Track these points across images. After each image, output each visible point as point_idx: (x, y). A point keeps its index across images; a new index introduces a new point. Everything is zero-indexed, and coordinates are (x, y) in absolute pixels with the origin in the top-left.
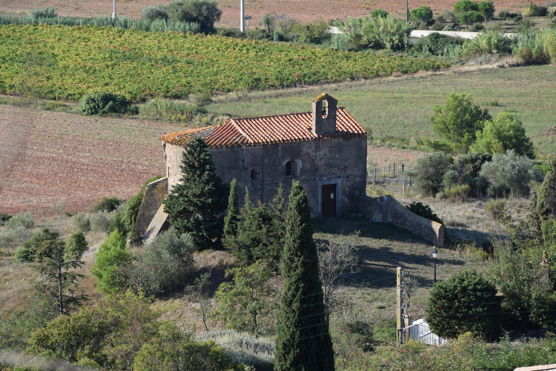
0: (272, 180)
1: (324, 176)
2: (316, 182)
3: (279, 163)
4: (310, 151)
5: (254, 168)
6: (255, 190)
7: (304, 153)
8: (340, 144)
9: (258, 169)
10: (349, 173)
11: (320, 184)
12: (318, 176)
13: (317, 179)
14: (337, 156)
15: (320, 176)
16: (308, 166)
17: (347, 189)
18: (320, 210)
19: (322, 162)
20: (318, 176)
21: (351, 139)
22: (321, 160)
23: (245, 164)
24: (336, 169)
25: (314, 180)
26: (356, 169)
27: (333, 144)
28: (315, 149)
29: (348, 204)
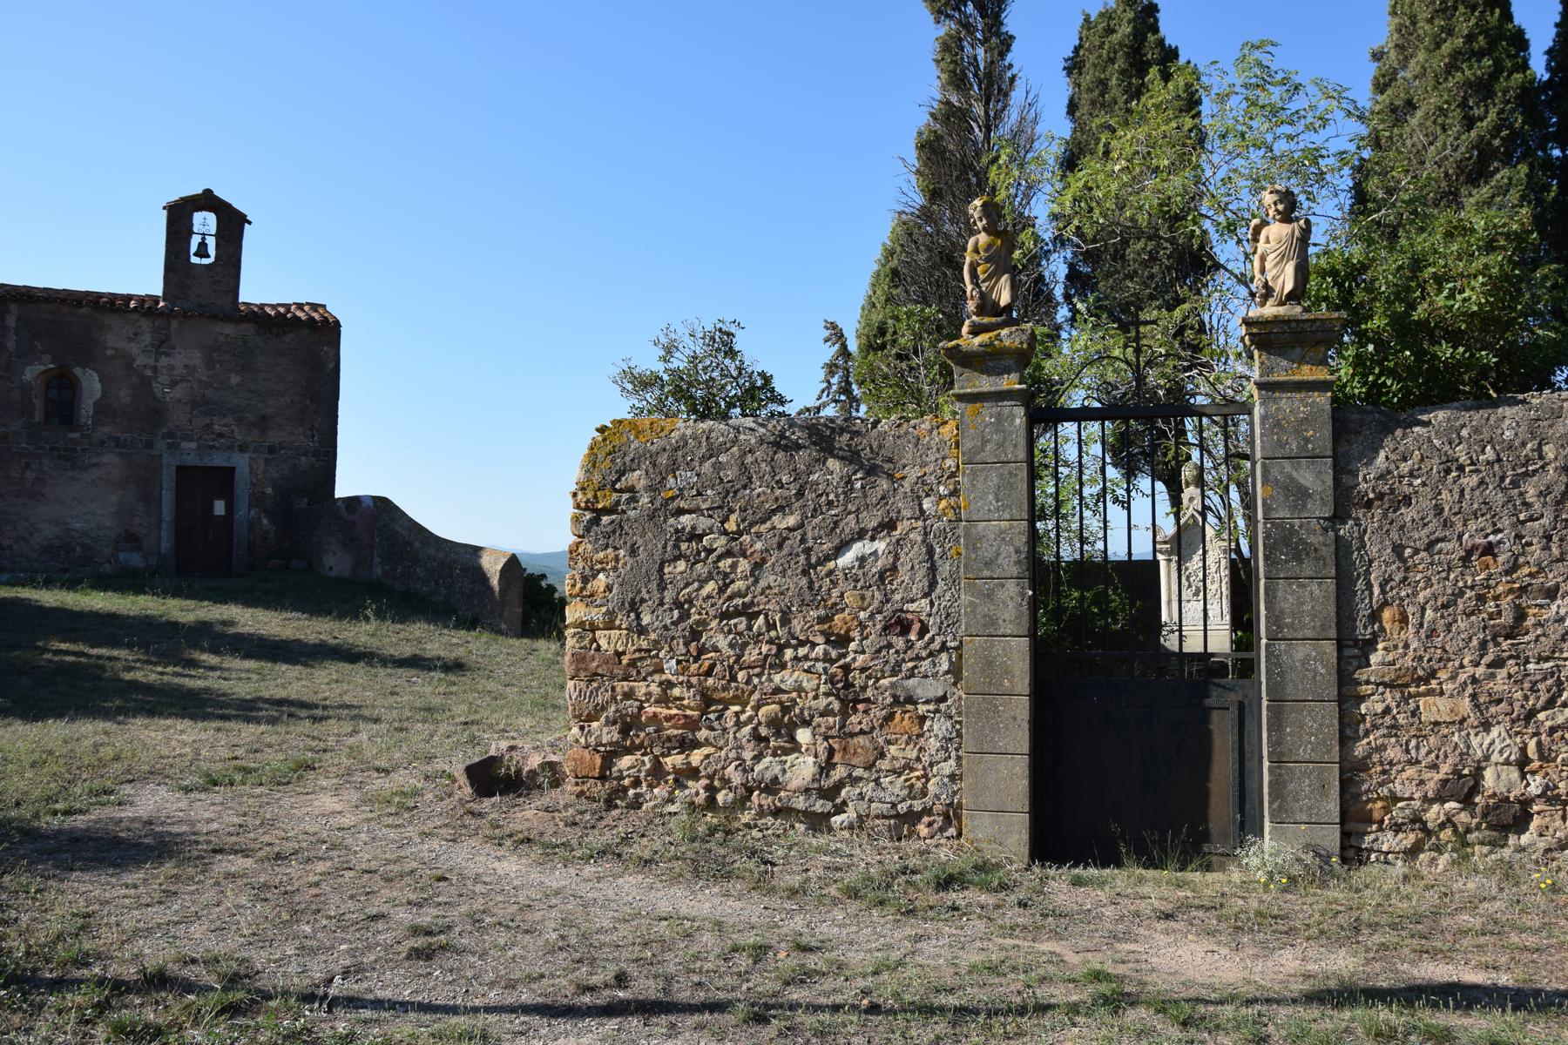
1: (188, 438)
4: (133, 348)
7: (109, 352)
8: (245, 343)
10: (274, 437)
11: (169, 462)
13: (160, 444)
14: (235, 379)
15: (171, 435)
16: (124, 395)
17: (269, 490)
18: (166, 545)
19: (180, 392)
22: (174, 384)
24: (230, 420)
25: (149, 445)
27: (221, 338)
28: (152, 345)
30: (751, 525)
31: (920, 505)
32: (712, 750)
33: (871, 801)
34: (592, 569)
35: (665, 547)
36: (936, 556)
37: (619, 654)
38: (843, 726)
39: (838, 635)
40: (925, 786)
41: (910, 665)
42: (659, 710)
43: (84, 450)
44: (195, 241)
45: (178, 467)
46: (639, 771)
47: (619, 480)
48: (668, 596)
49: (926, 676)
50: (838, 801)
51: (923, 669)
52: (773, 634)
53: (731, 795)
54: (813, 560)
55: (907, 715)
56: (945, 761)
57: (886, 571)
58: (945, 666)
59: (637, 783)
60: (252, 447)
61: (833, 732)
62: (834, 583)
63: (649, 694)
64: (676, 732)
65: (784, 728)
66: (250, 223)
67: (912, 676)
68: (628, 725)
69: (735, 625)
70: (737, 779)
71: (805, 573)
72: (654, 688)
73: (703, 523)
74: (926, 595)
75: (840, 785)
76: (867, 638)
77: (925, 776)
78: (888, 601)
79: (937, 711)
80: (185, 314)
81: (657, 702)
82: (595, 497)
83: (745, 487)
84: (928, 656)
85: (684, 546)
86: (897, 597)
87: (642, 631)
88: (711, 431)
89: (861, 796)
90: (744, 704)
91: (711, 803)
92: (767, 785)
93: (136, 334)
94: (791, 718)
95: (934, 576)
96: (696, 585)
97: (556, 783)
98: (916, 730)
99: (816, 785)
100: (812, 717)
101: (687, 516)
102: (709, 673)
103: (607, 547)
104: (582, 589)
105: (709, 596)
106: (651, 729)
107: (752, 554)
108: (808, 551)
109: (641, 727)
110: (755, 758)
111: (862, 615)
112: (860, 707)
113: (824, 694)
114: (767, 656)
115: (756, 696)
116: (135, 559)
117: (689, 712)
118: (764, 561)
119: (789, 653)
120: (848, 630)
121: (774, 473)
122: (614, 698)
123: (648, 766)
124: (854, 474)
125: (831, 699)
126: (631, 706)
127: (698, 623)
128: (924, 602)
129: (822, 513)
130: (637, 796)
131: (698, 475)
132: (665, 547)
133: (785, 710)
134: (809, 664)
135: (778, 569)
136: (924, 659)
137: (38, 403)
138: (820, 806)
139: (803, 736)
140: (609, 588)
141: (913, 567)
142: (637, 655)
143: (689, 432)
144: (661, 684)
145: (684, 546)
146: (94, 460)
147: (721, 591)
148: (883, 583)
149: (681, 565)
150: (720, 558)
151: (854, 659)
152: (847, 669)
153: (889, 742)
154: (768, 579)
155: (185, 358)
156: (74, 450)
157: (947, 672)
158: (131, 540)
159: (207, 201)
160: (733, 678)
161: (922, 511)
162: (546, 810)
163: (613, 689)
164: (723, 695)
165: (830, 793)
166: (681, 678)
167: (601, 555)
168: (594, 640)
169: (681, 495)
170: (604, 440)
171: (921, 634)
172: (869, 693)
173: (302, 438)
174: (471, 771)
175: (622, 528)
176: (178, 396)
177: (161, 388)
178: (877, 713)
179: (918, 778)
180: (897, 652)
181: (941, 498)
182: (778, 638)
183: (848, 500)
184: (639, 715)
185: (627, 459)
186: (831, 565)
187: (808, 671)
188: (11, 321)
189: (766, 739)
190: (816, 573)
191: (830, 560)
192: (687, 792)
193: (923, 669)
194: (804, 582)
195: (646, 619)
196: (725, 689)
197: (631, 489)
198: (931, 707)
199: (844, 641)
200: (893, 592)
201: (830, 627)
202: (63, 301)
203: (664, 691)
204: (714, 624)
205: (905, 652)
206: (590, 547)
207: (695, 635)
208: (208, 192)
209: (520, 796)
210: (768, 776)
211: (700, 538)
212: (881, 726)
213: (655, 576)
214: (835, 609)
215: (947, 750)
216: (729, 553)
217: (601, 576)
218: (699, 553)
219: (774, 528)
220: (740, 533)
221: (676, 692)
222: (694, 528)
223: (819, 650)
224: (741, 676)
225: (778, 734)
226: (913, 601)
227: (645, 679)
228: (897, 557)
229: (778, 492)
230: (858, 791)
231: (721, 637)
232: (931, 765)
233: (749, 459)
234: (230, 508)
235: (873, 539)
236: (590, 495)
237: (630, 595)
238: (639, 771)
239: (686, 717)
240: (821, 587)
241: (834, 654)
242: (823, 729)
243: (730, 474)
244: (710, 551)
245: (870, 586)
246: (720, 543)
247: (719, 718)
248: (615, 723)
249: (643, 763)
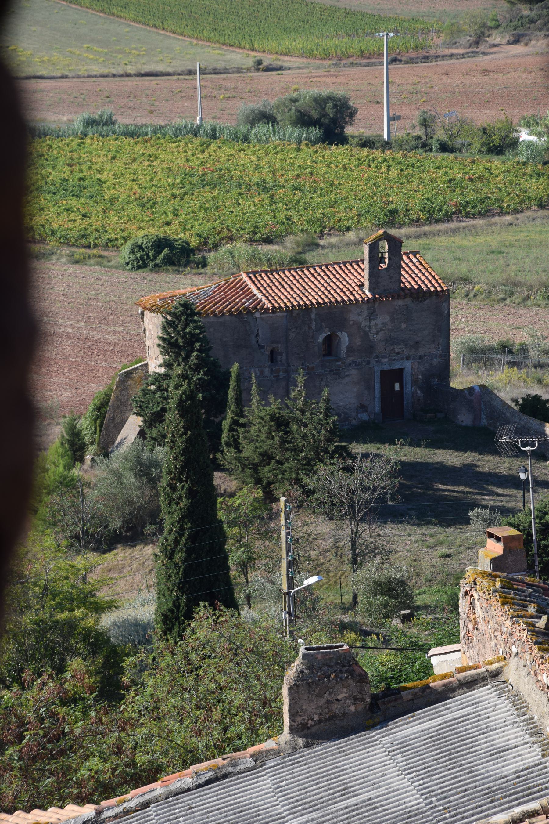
1: (384, 357)
2: (371, 366)
4: (361, 319)
5: (275, 345)
7: (351, 323)
8: (407, 307)
9: (280, 348)
11: (377, 369)
12: (375, 357)
13: (373, 361)
14: (404, 326)
15: (377, 356)
16: (358, 341)
17: (420, 377)
18: (378, 409)
19: (380, 336)
21: (425, 300)
22: (378, 332)
23: (260, 340)
24: (402, 346)
25: (368, 363)
26: (433, 345)
27: (397, 307)
28: (368, 316)
43: (343, 369)
146: (347, 373)
158: (362, 407)
173: (434, 350)
234: (401, 387)
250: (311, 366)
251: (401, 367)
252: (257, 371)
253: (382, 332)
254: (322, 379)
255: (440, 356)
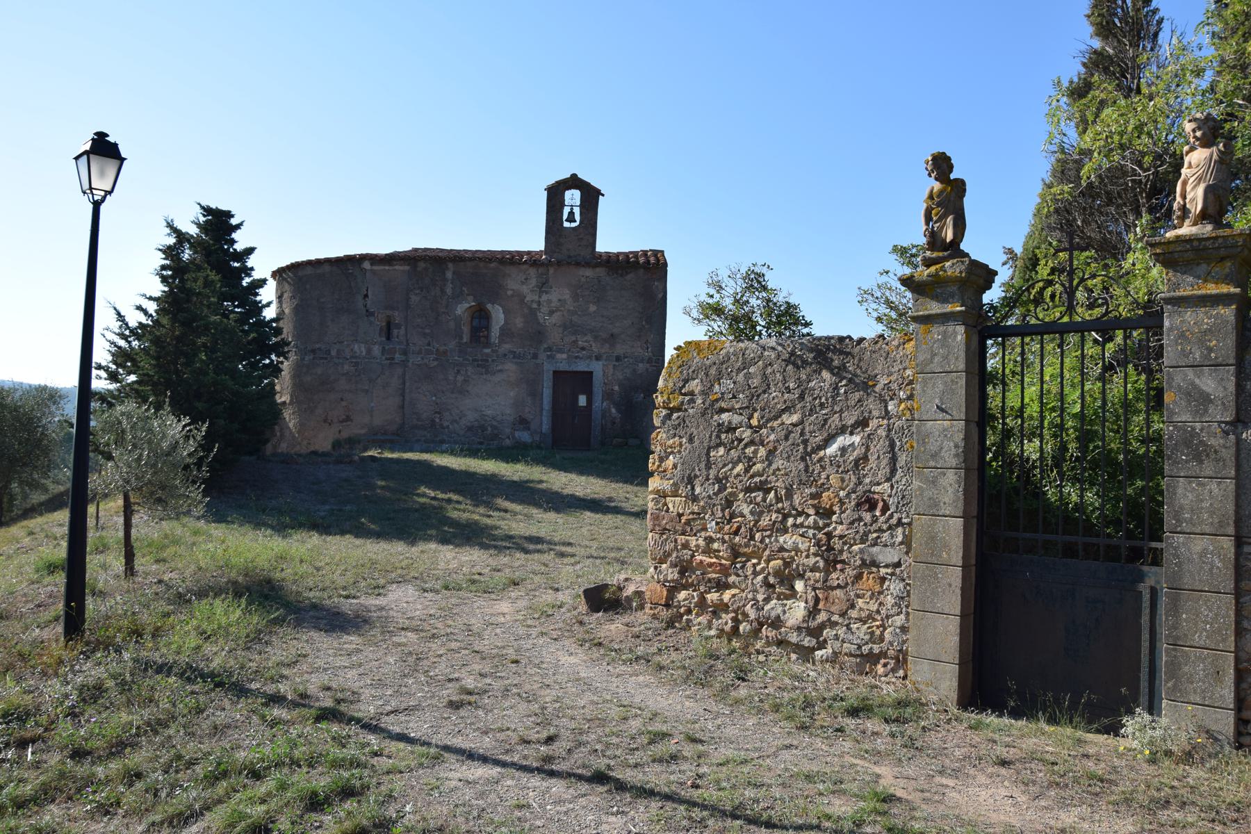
0: (429, 344)
1: (560, 351)
2: (538, 361)
3: (447, 307)
4: (525, 289)
6: (391, 364)
7: (509, 293)
9: (398, 317)
10: (620, 350)
11: (548, 368)
12: (546, 350)
13: (543, 356)
14: (593, 308)
15: (549, 349)
16: (519, 322)
17: (616, 388)
18: (546, 427)
19: (556, 318)
20: (546, 350)
21: (627, 273)
22: (551, 313)
24: (589, 337)
25: (535, 356)
26: (639, 343)
27: (583, 279)
28: (537, 286)
29: (618, 421)
30: (769, 420)
31: (886, 407)
32: (737, 591)
33: (843, 641)
34: (665, 452)
35: (710, 437)
36: (897, 448)
37: (680, 515)
38: (825, 581)
39: (825, 508)
40: (882, 633)
41: (875, 535)
42: (704, 558)
43: (493, 361)
44: (566, 211)
45: (555, 372)
46: (690, 603)
47: (684, 386)
48: (712, 473)
49: (886, 546)
50: (821, 639)
51: (883, 539)
52: (780, 505)
53: (748, 627)
54: (809, 449)
55: (872, 576)
56: (898, 615)
57: (860, 459)
58: (900, 539)
59: (689, 611)
60: (605, 356)
61: (819, 585)
62: (823, 468)
63: (697, 546)
64: (714, 576)
65: (786, 579)
66: (603, 195)
67: (875, 544)
68: (685, 568)
69: (755, 497)
70: (752, 614)
71: (803, 459)
72: (701, 542)
73: (736, 419)
74: (888, 480)
75: (822, 627)
76: (844, 512)
77: (882, 626)
78: (860, 483)
79: (892, 574)
80: (559, 263)
81: (703, 552)
82: (669, 398)
83: (764, 392)
84: (888, 529)
85: (723, 436)
86: (867, 480)
87: (695, 499)
88: (746, 349)
89: (837, 637)
90: (760, 559)
91: (735, 629)
92: (772, 622)
93: (526, 279)
94: (789, 572)
95: (895, 464)
96: (730, 465)
97: (641, 607)
98: (877, 588)
99: (805, 625)
100: (805, 571)
101: (727, 414)
102: (736, 533)
103: (675, 436)
104: (659, 466)
105: (738, 475)
106: (698, 573)
107: (768, 443)
108: (805, 442)
109: (693, 571)
110: (764, 600)
111: (842, 493)
112: (839, 566)
113: (813, 554)
114: (775, 522)
115: (767, 553)
116: (525, 436)
117: (723, 562)
118: (775, 449)
119: (790, 521)
120: (832, 505)
121: (785, 381)
122: (676, 547)
123: (696, 599)
124: (840, 381)
125: (818, 558)
126: (686, 554)
127: (731, 494)
128: (887, 485)
129: (816, 413)
130: (689, 621)
131: (734, 383)
132: (710, 437)
133: (787, 564)
134: (804, 530)
135: (785, 455)
136: (885, 531)
137: (466, 330)
138: (808, 642)
139: (799, 586)
140: (675, 466)
141: (879, 457)
142: (691, 517)
143: (732, 350)
144: (706, 539)
145: (723, 436)
146: (499, 368)
147: (747, 470)
148: (857, 469)
149: (721, 451)
150: (746, 446)
151: (835, 529)
152: (829, 536)
153: (858, 596)
154: (778, 463)
155: (559, 294)
156: (487, 361)
157: (901, 543)
158: (523, 422)
159: (574, 182)
160: (752, 538)
161: (887, 412)
162: (627, 625)
163: (676, 541)
164: (746, 550)
165: (815, 632)
166: (718, 536)
167: (671, 441)
168: (665, 504)
169: (722, 398)
170: (678, 356)
171: (883, 513)
172: (845, 556)
174: (587, 593)
175: (684, 422)
176: (554, 321)
177: (543, 317)
178: (850, 572)
179: (878, 627)
180: (865, 524)
181: (901, 401)
182: (783, 509)
183: (834, 403)
184: (690, 561)
185: (691, 370)
186: (822, 453)
187: (802, 536)
188: (449, 275)
189: (773, 586)
190: (811, 459)
191: (821, 450)
192: (720, 621)
193: (883, 539)
194: (802, 466)
195: (698, 490)
196: (747, 545)
197: (692, 393)
198: (889, 571)
199: (828, 513)
200: (864, 476)
201: (819, 502)
202: (470, 259)
203: (708, 544)
204: (741, 496)
205: (871, 525)
206: (664, 435)
207: (729, 503)
208: (574, 176)
209: (617, 613)
210: (773, 614)
211: (735, 429)
212: (853, 583)
213: (704, 458)
214: (824, 488)
215: (900, 607)
216: (752, 443)
217: (671, 457)
218: (733, 442)
219: (783, 424)
220: (760, 427)
221: (716, 546)
222: (730, 423)
223: (811, 519)
224: (758, 536)
225: (781, 583)
226: (878, 484)
227: (695, 535)
228: (868, 449)
229: (786, 396)
230: (835, 632)
231: (745, 505)
232: (888, 617)
233: (769, 370)
234: (589, 401)
235: (852, 434)
236: (665, 398)
237: (688, 472)
238: (690, 603)
239: (721, 564)
240: (813, 470)
241: (821, 523)
242: (812, 582)
243: (755, 382)
244: (740, 440)
245: (848, 471)
246: (747, 434)
247: (742, 567)
248: (676, 566)
249: (693, 596)
250: (442, 348)
251: (586, 370)
252: (363, 349)
253: (559, 313)
254: (458, 371)
255: (649, 361)
